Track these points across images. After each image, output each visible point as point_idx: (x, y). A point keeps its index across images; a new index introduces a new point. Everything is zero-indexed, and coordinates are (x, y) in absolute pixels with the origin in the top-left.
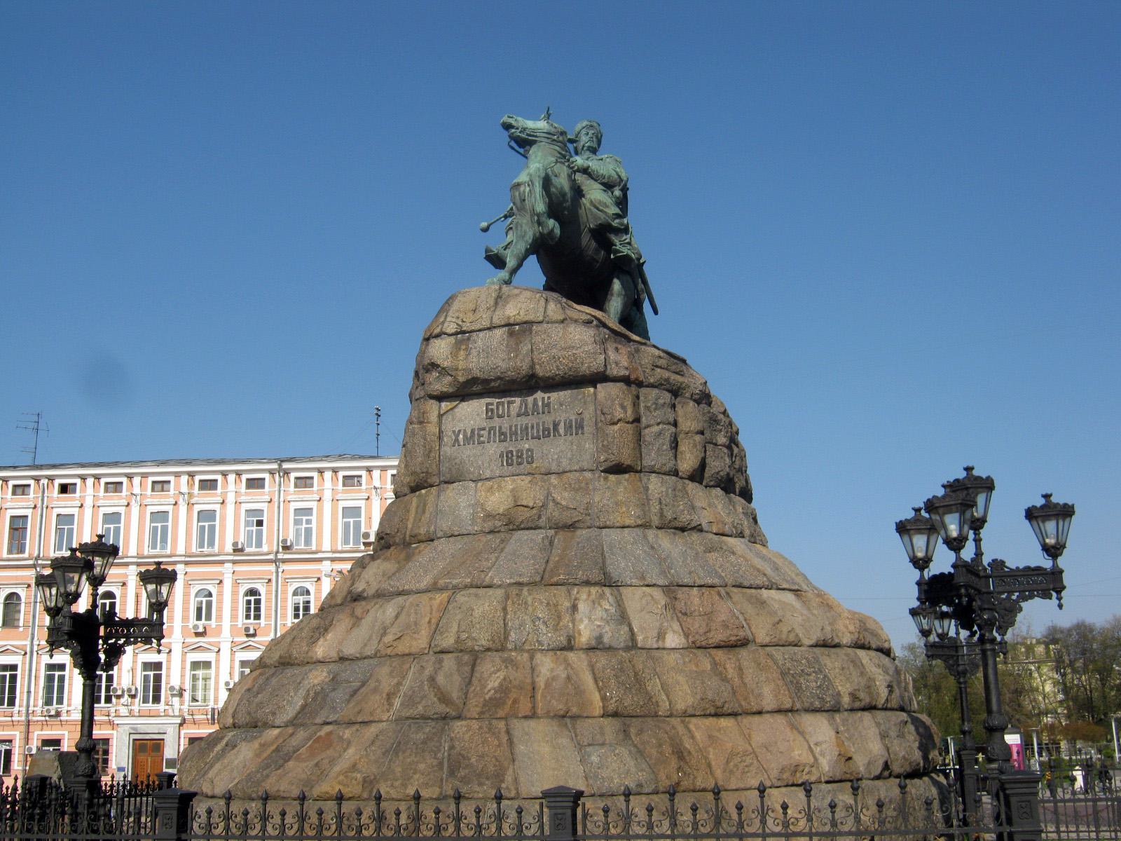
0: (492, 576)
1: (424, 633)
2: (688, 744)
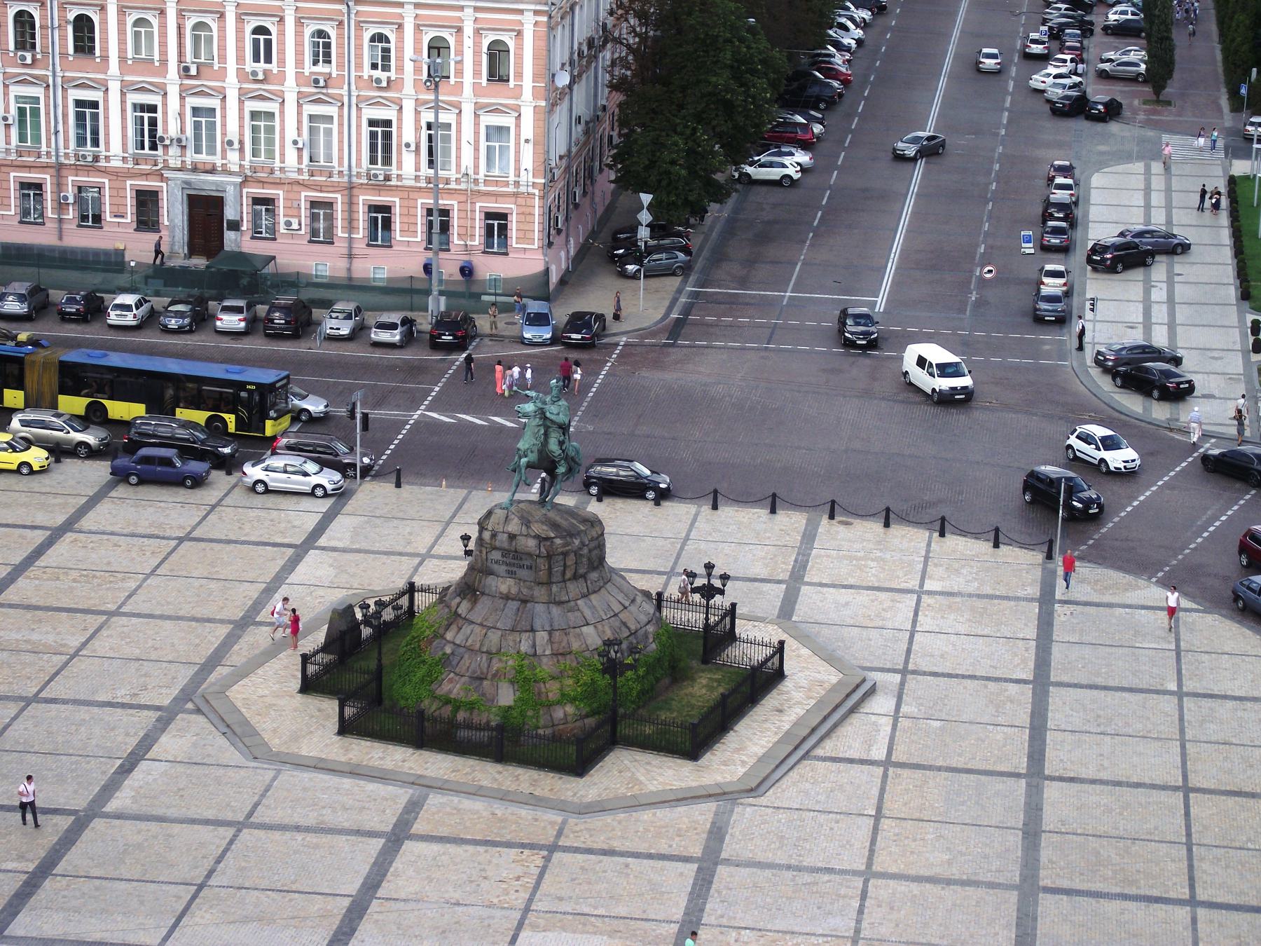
0: (498, 625)
1: (478, 645)
2: (543, 690)
